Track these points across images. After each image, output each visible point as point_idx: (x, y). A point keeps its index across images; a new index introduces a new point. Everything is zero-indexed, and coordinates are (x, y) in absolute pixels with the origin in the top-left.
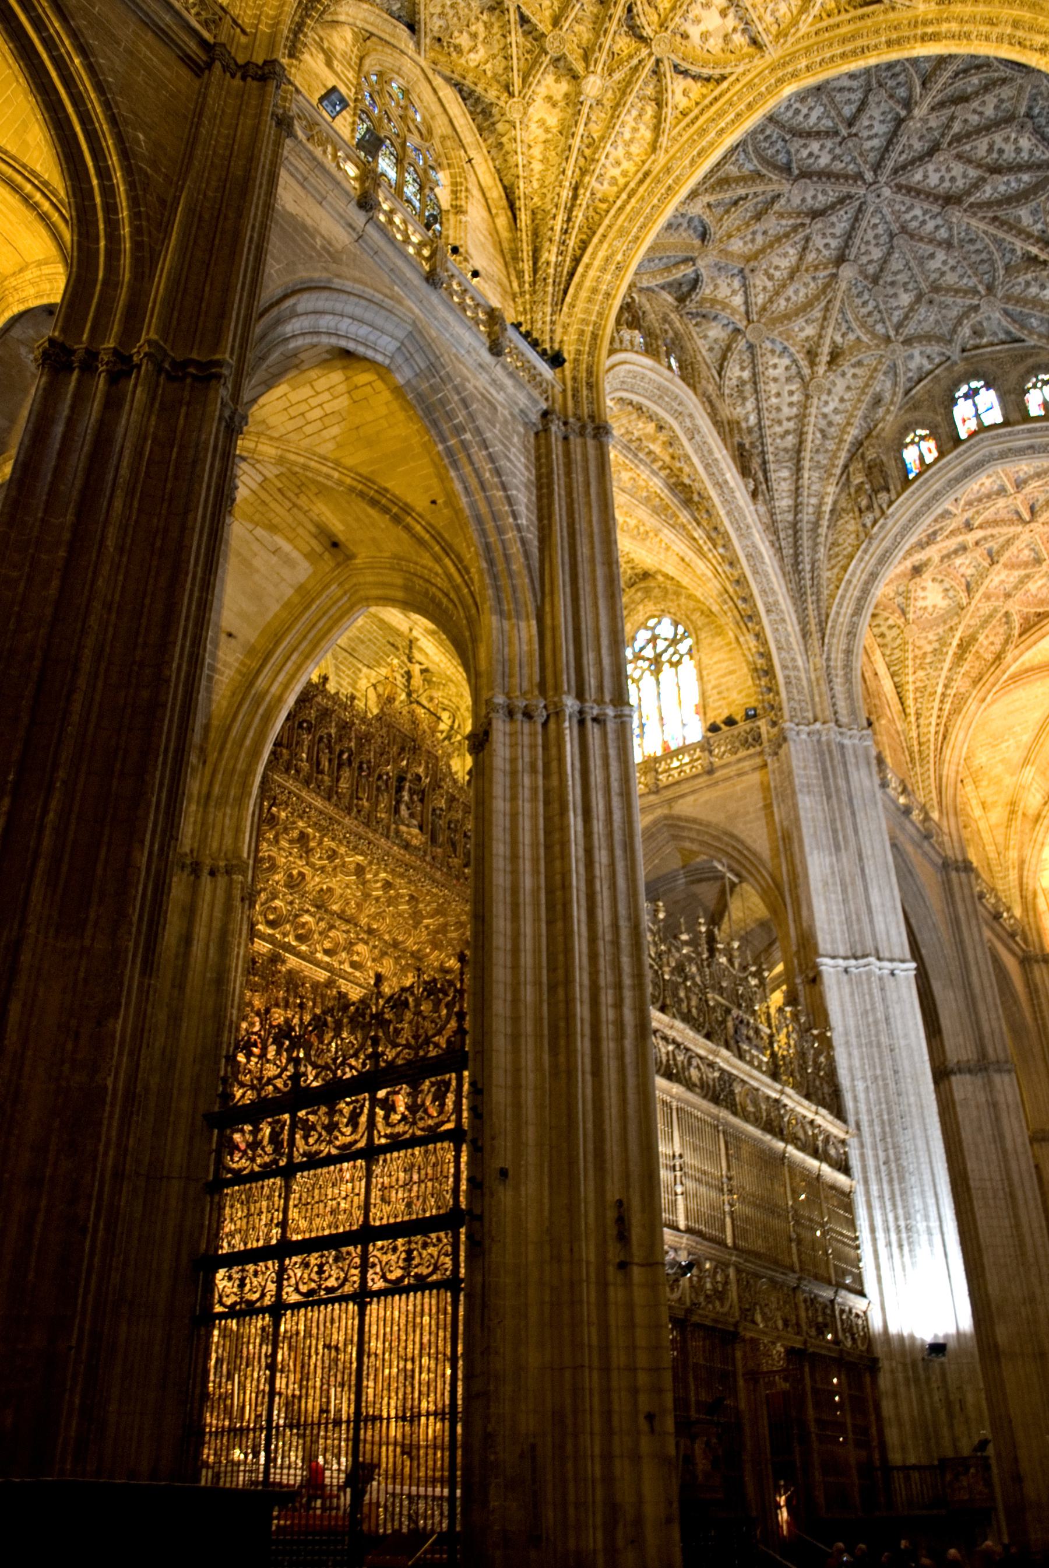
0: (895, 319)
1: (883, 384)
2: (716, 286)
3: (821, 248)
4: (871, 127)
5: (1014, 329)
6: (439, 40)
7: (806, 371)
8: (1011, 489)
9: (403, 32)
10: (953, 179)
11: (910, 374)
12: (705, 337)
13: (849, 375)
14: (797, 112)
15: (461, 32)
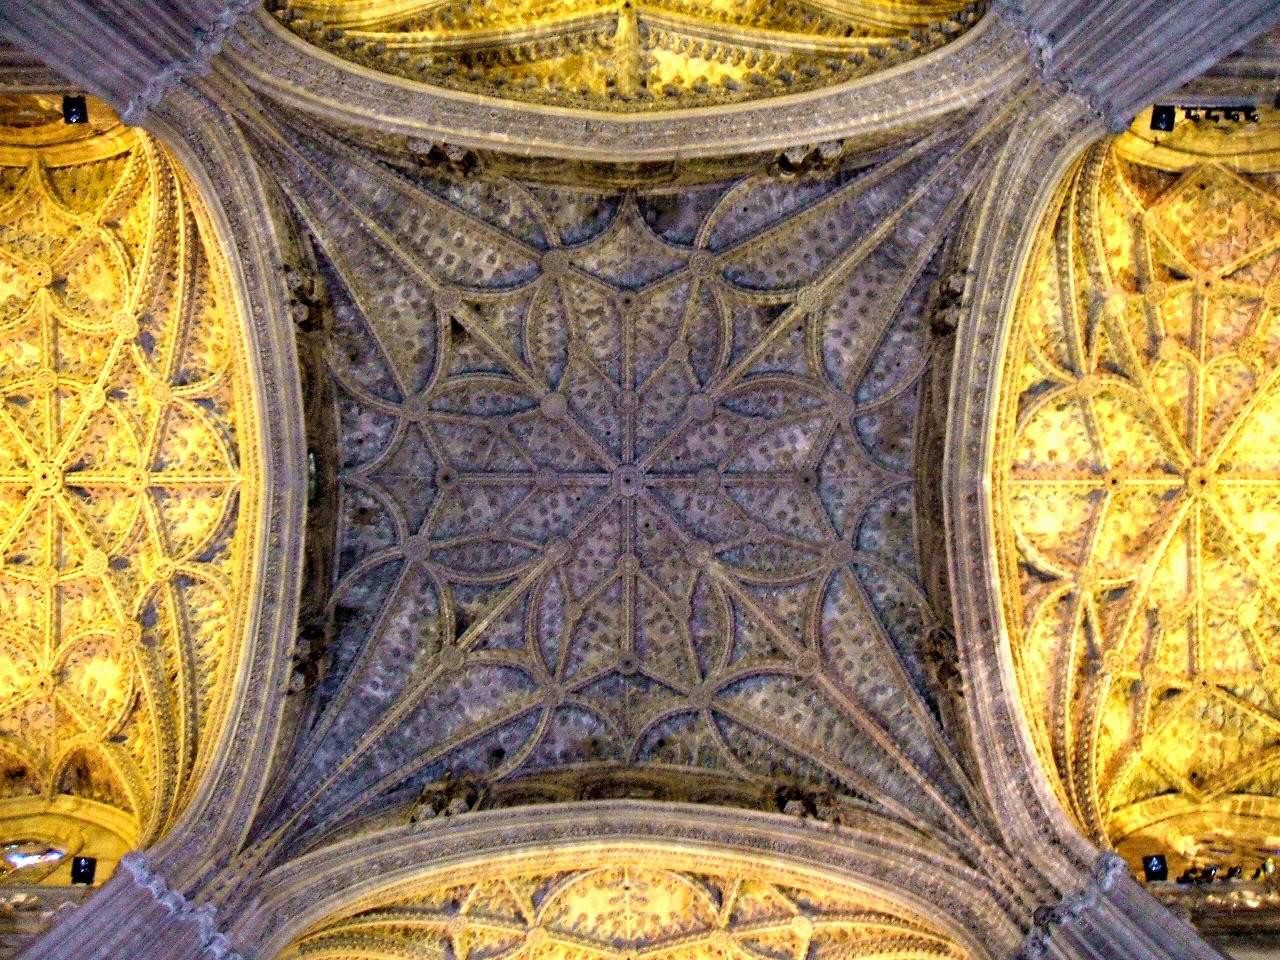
0: (440, 426)
1: (368, 374)
2: (622, 248)
3: (583, 386)
4: (702, 507)
5: (366, 564)
6: (1203, 187)
7: (473, 296)
8: (160, 479)
9: (1253, 168)
10: (584, 564)
11: (355, 410)
12: (570, 199)
13: (416, 340)
14: (779, 444)
15: (1195, 211)
